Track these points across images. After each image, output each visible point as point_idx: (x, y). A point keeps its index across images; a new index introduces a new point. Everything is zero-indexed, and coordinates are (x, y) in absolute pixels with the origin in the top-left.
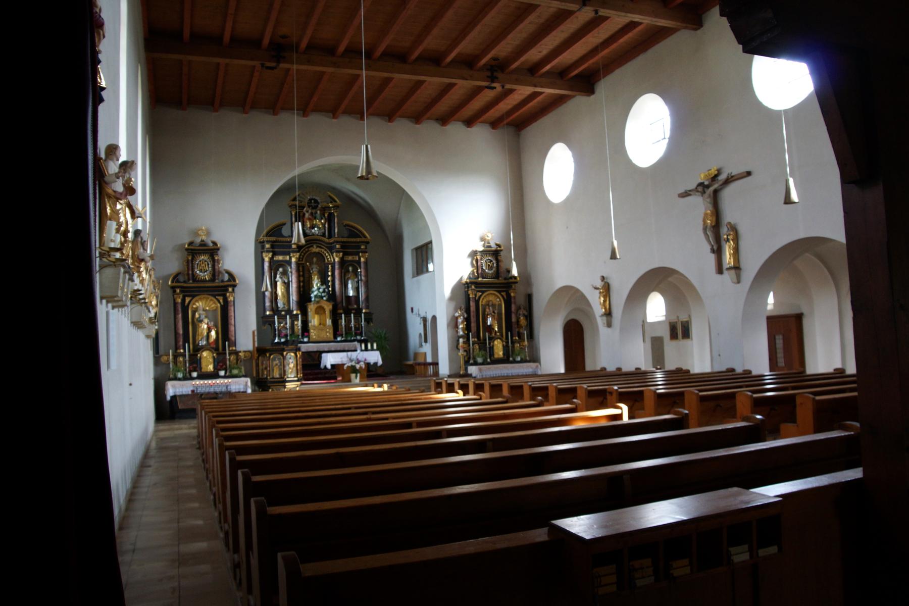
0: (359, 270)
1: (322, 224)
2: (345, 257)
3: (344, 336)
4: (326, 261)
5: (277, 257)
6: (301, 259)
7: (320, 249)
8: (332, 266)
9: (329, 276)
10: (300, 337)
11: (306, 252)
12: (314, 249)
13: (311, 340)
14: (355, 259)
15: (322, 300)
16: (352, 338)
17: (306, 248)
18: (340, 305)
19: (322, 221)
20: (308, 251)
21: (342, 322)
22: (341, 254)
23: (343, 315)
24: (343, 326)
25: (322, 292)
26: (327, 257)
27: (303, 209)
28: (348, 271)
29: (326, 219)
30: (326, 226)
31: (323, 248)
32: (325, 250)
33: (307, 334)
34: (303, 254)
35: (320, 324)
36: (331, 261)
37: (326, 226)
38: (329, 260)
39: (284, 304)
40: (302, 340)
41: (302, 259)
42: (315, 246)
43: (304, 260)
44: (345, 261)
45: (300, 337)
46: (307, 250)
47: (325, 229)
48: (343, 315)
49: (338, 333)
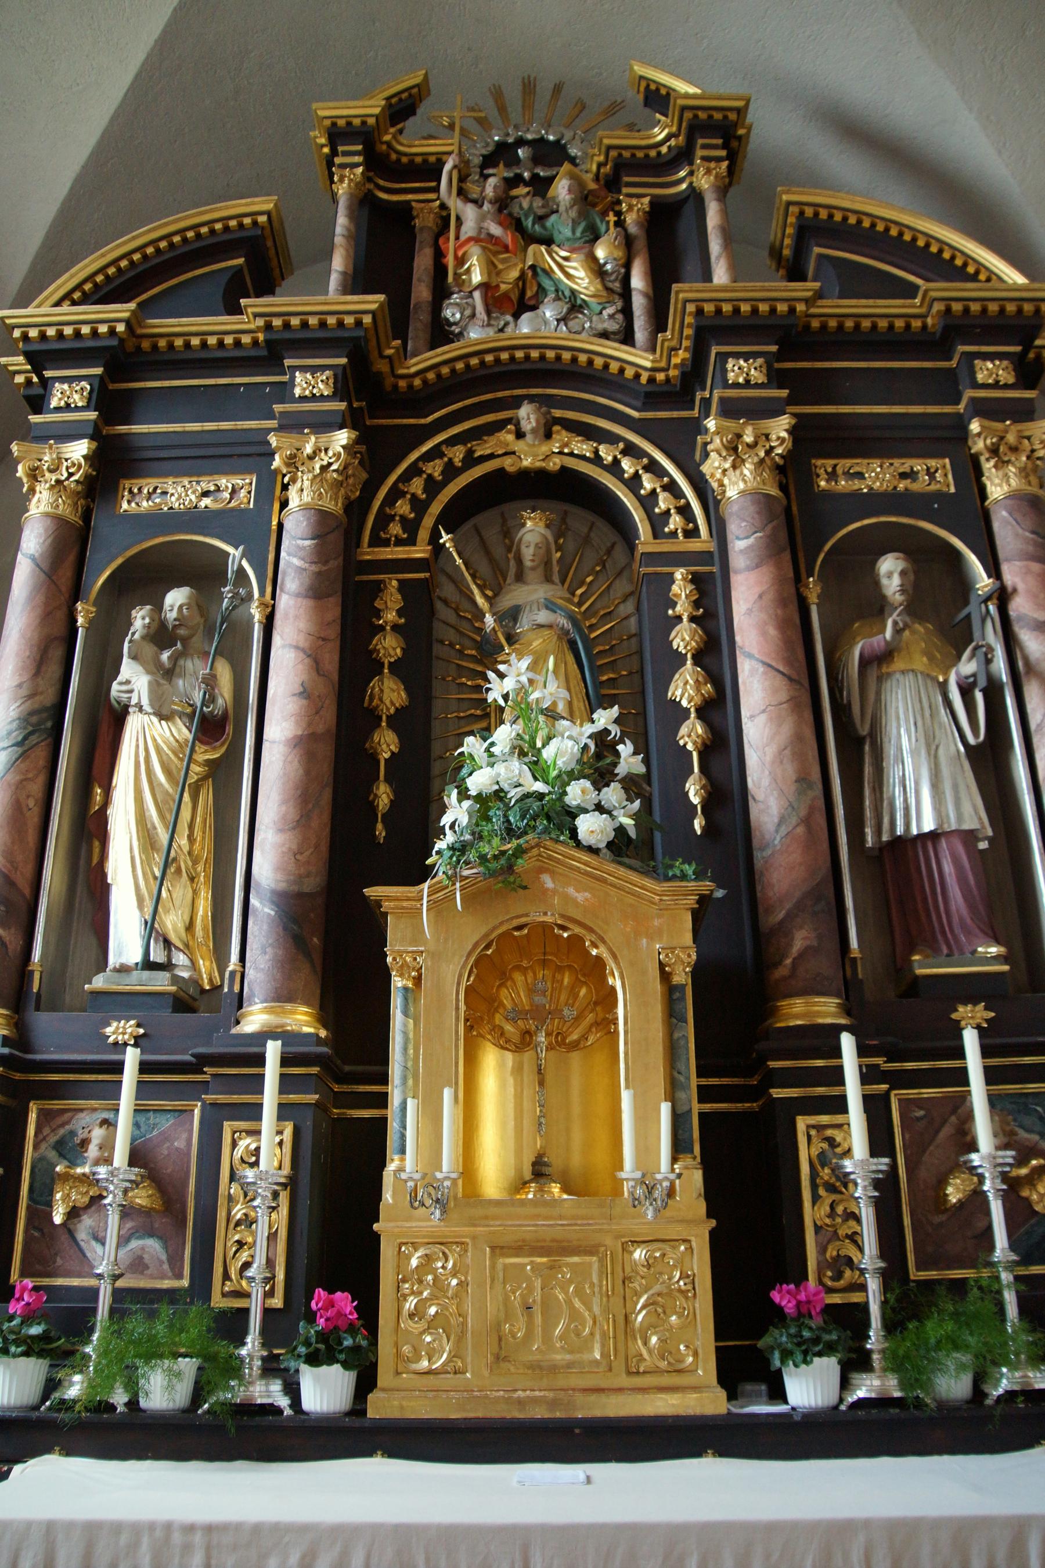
0: (983, 582)
1: (598, 271)
2: (823, 465)
3: (875, 1339)
4: (643, 529)
5: (148, 484)
6: (395, 529)
7: (583, 447)
8: (696, 580)
9: (678, 660)
10: (251, 1347)
11: (451, 472)
12: (519, 446)
13: (381, 1405)
14: (922, 484)
15: (564, 850)
16: (1005, 1382)
17: (452, 441)
18: (801, 940)
19: (601, 253)
20: (471, 461)
21: (840, 1150)
22: (780, 428)
23: (847, 1042)
24: (862, 1191)
25: (572, 776)
26: (648, 502)
27: (436, 189)
28: (878, 607)
29: (629, 243)
30: (637, 282)
31: (611, 439)
32: (631, 450)
33: (345, 1301)
34: (417, 486)
35: (540, 1171)
36: (692, 533)
37: (637, 282)
38: (676, 522)
39: (151, 929)
40: (271, 1393)
41: (411, 527)
42: (527, 415)
43: (424, 534)
44: (826, 494)
45: (251, 1347)
46: (457, 454)
47: (627, 311)
48: (847, 1042)
49: (782, 1297)
